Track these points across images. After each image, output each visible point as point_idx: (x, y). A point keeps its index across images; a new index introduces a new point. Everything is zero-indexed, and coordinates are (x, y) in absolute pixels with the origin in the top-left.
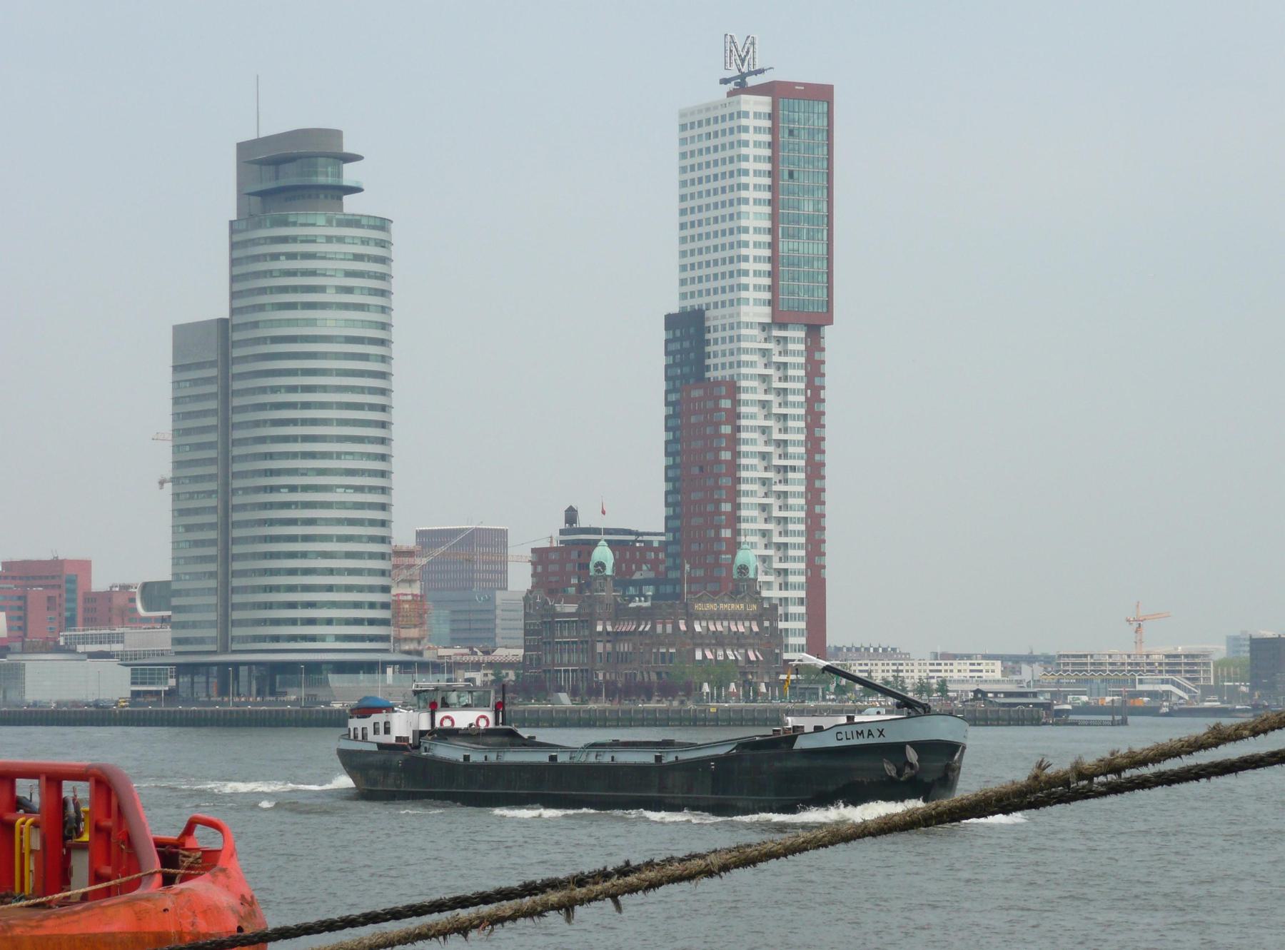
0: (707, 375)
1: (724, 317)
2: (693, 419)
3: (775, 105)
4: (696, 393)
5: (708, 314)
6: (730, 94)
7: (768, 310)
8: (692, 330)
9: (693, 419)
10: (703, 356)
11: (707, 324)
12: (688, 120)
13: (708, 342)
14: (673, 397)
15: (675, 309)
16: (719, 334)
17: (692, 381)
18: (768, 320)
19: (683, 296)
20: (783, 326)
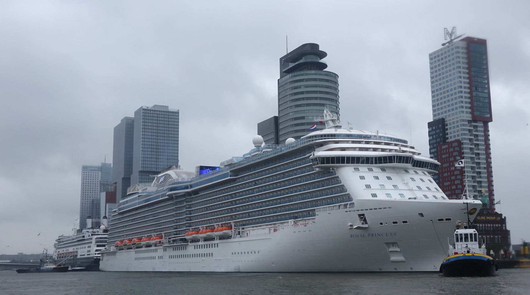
0: (447, 141)
1: (454, 119)
2: (443, 156)
4: (444, 147)
5: (446, 120)
7: (470, 115)
8: (440, 126)
9: (443, 156)
11: (446, 123)
12: (433, 56)
13: (447, 129)
14: (433, 151)
15: (432, 120)
16: (452, 126)
17: (441, 143)
19: (434, 116)
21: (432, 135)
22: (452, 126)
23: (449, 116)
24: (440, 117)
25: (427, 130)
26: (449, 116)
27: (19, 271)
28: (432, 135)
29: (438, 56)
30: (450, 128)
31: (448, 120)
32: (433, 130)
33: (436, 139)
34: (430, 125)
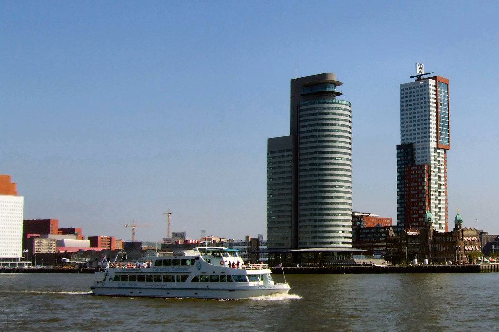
3: (436, 83)
6: (416, 81)
10: (413, 157)
12: (405, 87)
15: (400, 144)
18: (436, 147)
19: (403, 140)
20: (439, 149)
21: (401, 157)
22: (420, 151)
23: (418, 142)
24: (409, 141)
25: (395, 151)
26: (418, 142)
27: (230, 291)
28: (401, 157)
29: (410, 88)
30: (419, 153)
31: (416, 146)
32: (401, 152)
33: (404, 160)
34: (398, 147)
